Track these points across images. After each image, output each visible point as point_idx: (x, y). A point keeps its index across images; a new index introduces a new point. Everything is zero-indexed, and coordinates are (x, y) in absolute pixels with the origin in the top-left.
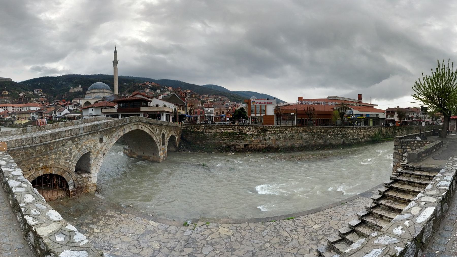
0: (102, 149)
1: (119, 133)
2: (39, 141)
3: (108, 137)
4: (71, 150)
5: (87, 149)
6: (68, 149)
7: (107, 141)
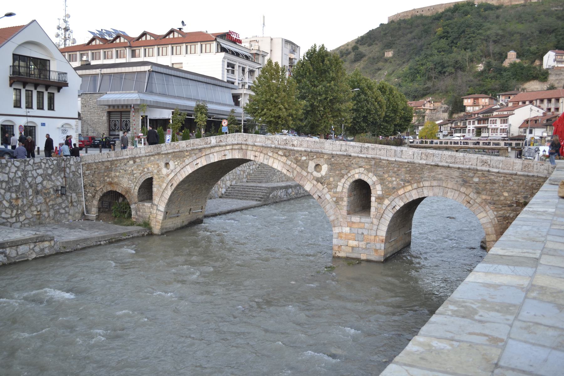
1: (198, 161)
3: (176, 163)
4: (133, 171)
6: (130, 169)
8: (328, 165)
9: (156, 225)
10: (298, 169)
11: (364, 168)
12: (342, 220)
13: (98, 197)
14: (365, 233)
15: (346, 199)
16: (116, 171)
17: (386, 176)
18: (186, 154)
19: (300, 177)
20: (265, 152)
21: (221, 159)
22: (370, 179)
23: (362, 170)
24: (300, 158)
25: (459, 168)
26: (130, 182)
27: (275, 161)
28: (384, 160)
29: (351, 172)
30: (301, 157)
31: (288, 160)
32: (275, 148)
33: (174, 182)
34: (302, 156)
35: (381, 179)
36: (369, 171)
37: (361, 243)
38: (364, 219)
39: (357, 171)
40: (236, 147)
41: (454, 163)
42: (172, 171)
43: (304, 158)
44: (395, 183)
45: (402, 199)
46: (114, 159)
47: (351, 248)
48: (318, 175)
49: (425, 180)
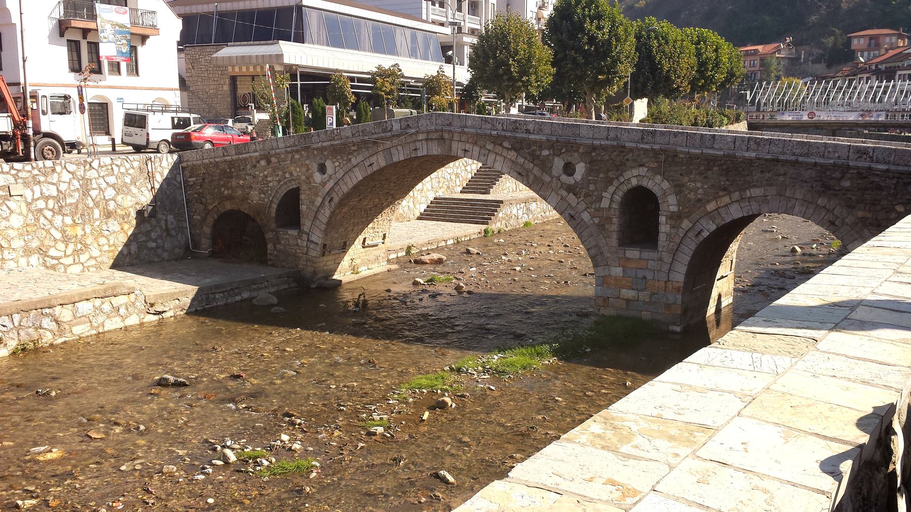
0: (323, 186)
1: (373, 159)
2: (222, 155)
3: (337, 164)
4: (266, 177)
5: (294, 180)
6: (261, 175)
7: (336, 173)
8: (585, 163)
9: (306, 265)
10: (536, 171)
11: (647, 167)
12: (609, 255)
13: (210, 220)
14: (649, 276)
15: (615, 220)
16: (238, 177)
17: (686, 179)
18: (353, 148)
19: (540, 185)
20: (481, 143)
21: (409, 157)
22: (657, 185)
23: (643, 171)
24: (538, 153)
25: (816, 164)
26: (262, 196)
27: (498, 158)
28: (682, 152)
29: (624, 174)
30: (541, 151)
31: (519, 156)
32: (498, 136)
33: (334, 195)
34: (542, 150)
35: (676, 186)
36: (656, 171)
37: (641, 294)
38: (647, 253)
39: (635, 172)
40: (434, 136)
41: (807, 155)
42: (330, 177)
43: (545, 153)
44: (700, 191)
45: (713, 219)
46: (235, 157)
47: (625, 302)
48: (570, 180)
49: (755, 186)
